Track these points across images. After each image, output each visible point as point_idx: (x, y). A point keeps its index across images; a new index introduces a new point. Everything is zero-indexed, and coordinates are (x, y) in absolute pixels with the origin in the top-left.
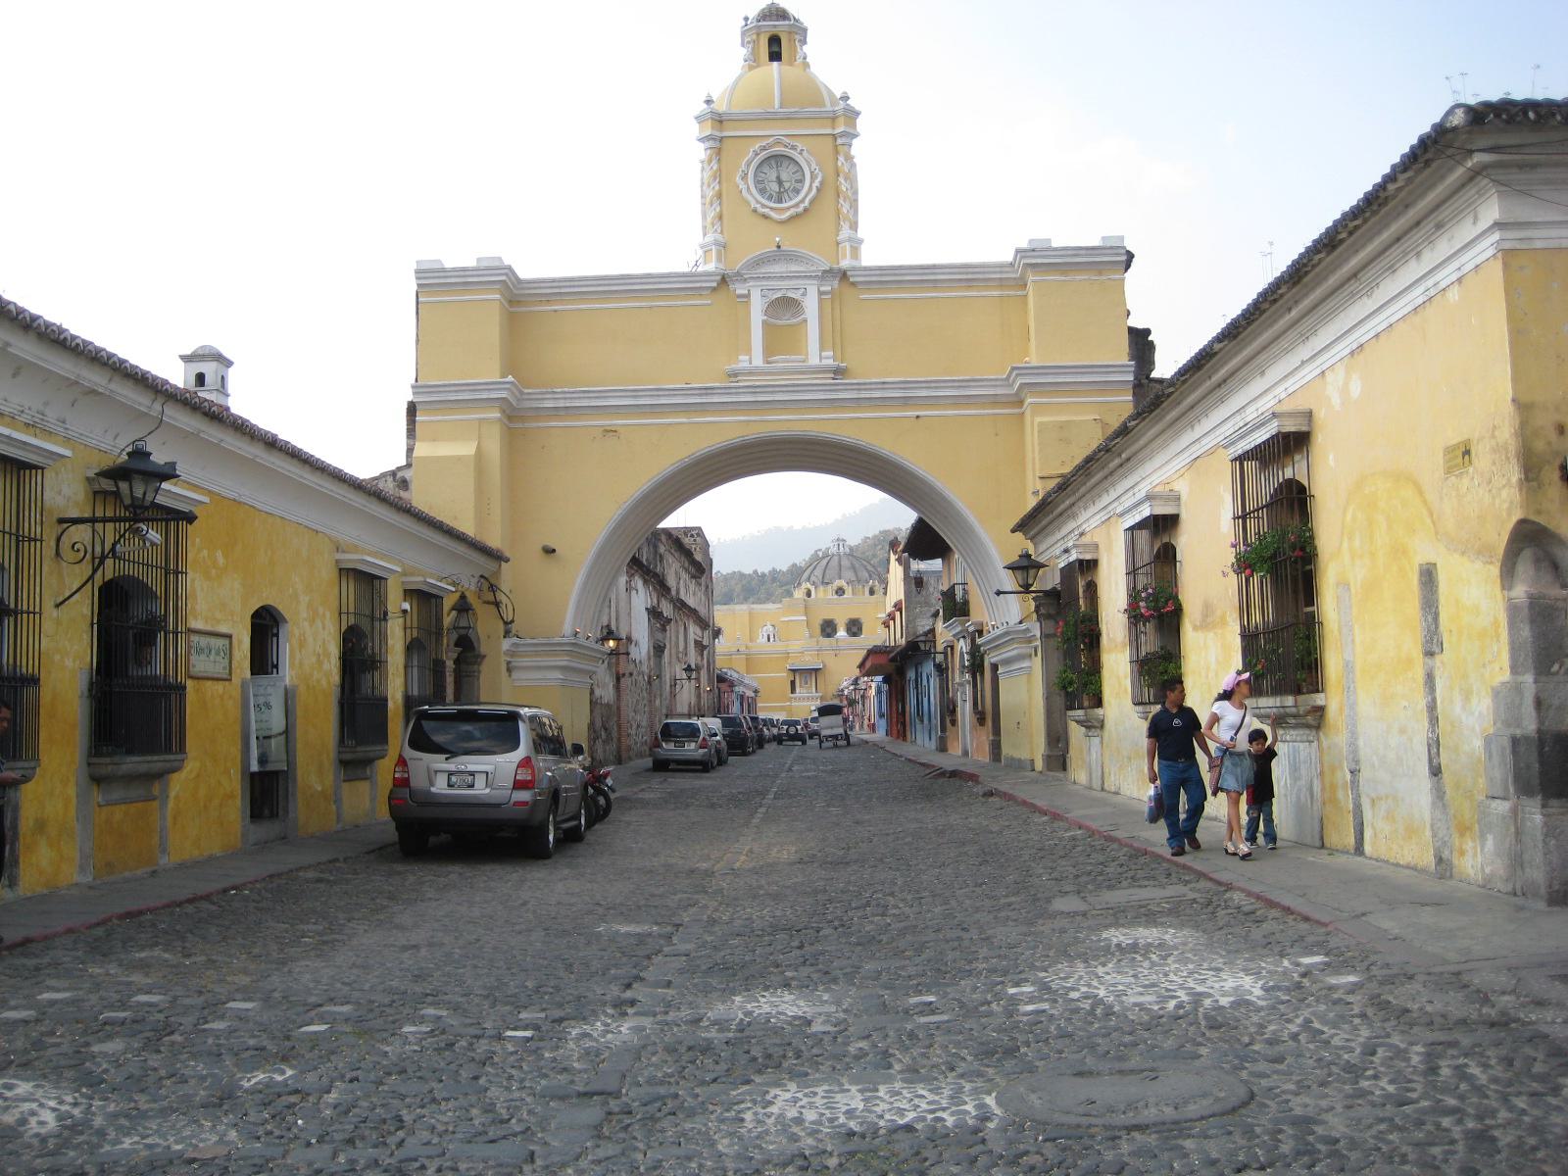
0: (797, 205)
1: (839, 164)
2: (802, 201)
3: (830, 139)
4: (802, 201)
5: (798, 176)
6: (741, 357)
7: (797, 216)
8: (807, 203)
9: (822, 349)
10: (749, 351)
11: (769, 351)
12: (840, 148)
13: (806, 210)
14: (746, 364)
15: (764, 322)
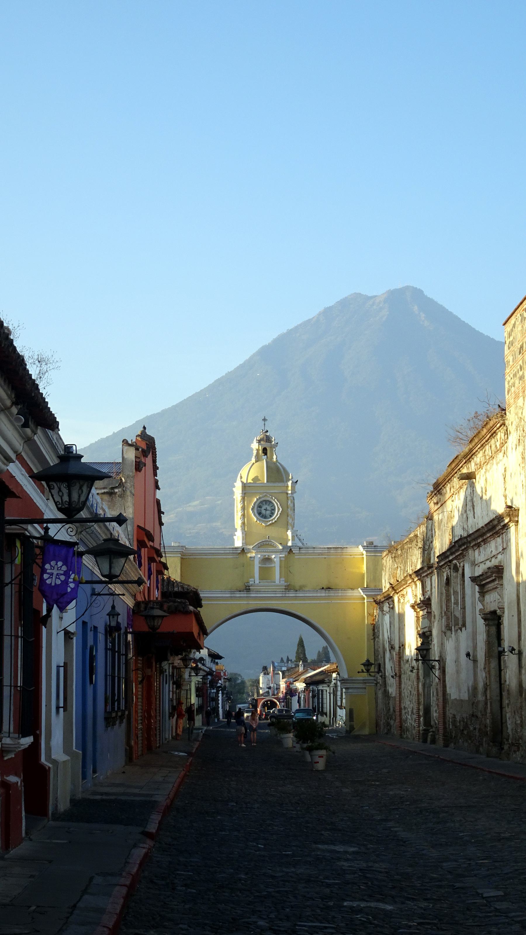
0: (272, 520)
1: (289, 504)
2: (274, 518)
3: (285, 494)
4: (274, 518)
5: (273, 508)
6: (250, 579)
7: (273, 523)
8: (276, 520)
9: (280, 577)
10: (254, 577)
11: (261, 578)
12: (289, 498)
13: (275, 521)
14: (253, 582)
15: (259, 567)
